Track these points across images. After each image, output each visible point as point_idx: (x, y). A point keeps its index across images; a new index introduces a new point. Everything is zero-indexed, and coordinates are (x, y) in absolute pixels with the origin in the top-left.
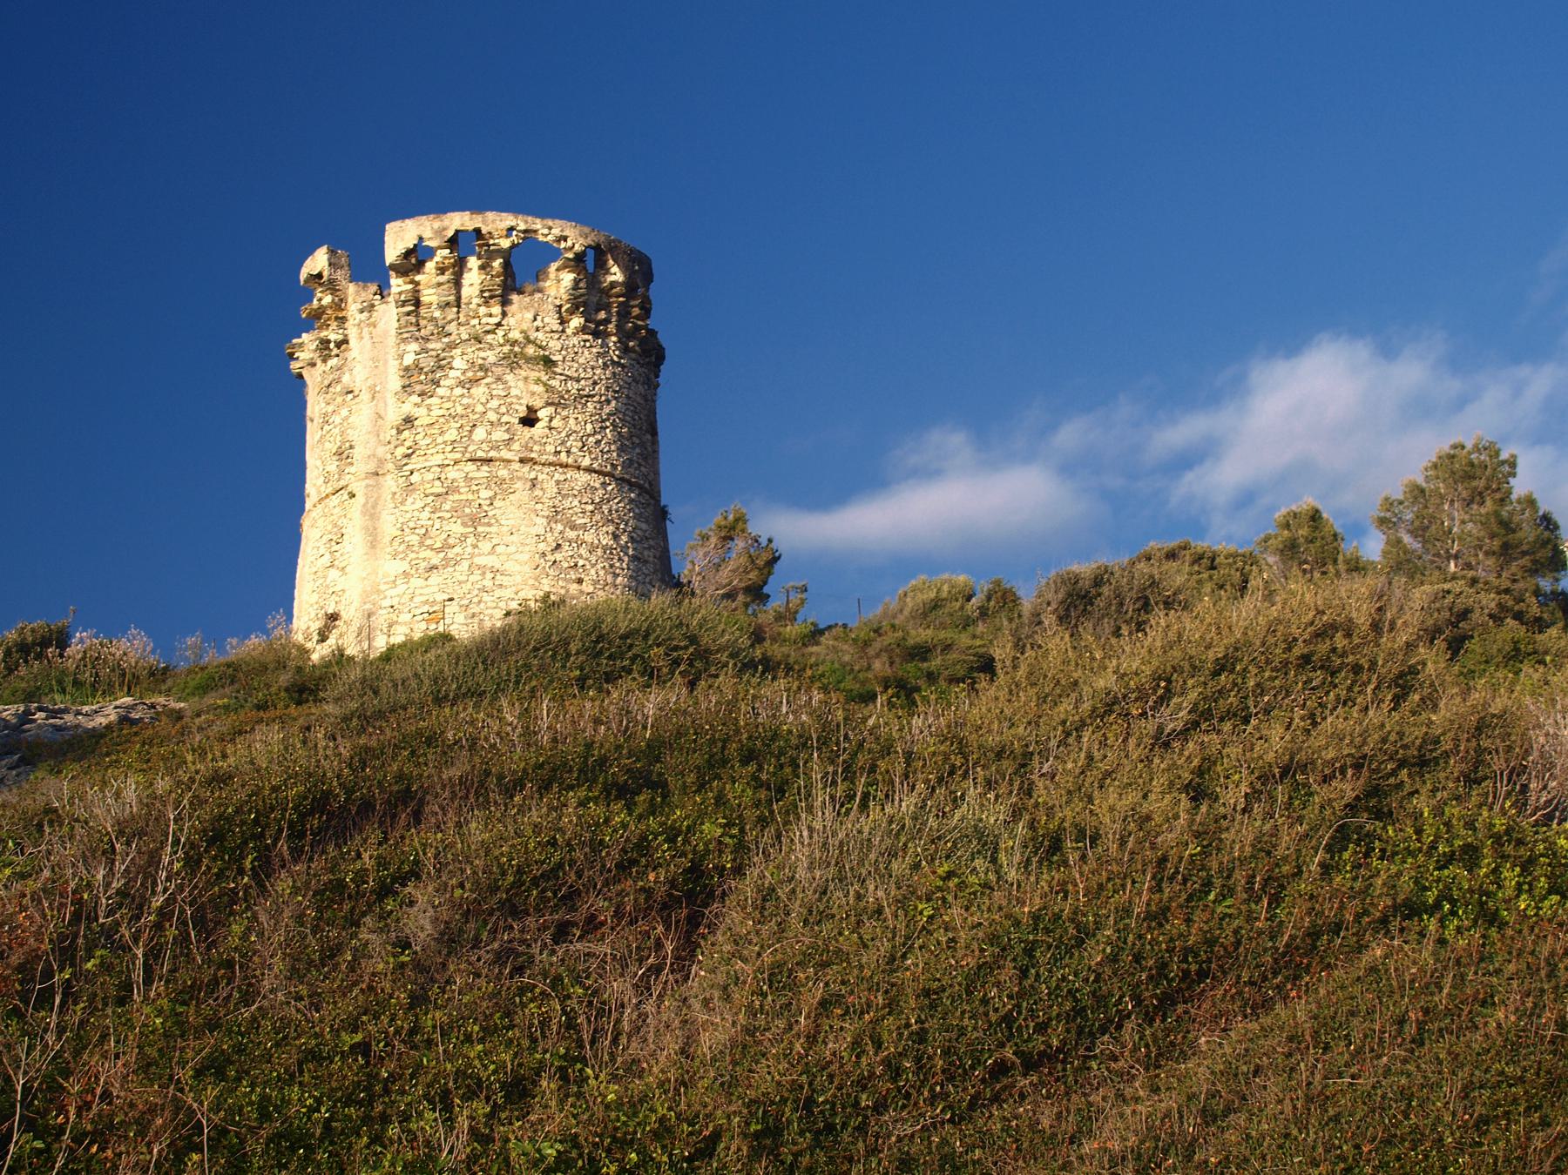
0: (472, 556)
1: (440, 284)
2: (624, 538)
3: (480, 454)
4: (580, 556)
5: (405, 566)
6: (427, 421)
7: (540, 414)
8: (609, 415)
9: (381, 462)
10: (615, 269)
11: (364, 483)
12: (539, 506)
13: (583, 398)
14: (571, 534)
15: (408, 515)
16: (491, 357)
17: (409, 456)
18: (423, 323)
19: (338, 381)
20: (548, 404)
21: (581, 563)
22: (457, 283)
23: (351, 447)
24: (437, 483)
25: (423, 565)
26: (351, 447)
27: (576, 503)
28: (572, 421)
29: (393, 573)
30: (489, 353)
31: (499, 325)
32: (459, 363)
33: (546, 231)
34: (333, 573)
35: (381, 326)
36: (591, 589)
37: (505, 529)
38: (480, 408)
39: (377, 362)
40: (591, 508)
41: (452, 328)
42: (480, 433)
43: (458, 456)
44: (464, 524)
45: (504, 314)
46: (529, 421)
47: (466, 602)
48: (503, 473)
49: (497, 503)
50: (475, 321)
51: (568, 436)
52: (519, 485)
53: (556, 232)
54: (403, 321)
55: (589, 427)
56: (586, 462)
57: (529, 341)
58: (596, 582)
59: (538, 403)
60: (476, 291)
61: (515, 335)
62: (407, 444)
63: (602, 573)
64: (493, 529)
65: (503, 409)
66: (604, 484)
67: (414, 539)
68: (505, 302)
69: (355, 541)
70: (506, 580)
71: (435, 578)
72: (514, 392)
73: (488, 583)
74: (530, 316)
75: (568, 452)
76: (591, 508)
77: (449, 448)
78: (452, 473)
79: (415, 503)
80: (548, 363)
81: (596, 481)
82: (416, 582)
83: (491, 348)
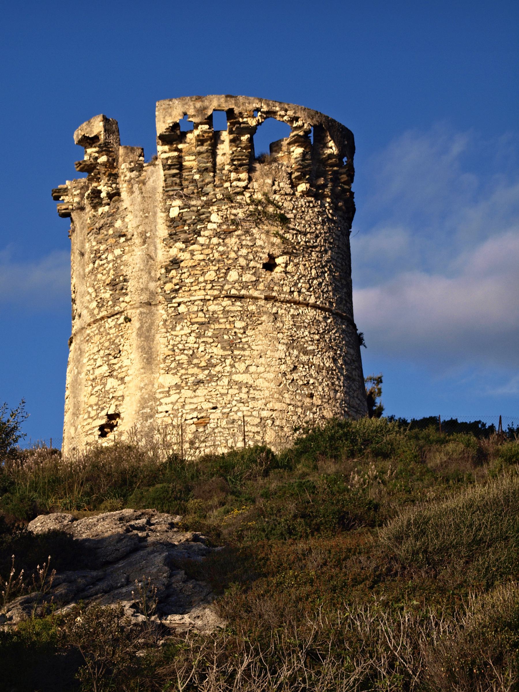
0: (231, 373)
1: (200, 153)
2: (340, 362)
3: (233, 292)
4: (311, 376)
5: (176, 380)
6: (191, 263)
7: (278, 261)
8: (327, 262)
9: (153, 294)
10: (331, 144)
11: (138, 311)
12: (280, 335)
13: (308, 248)
14: (304, 358)
15: (178, 339)
16: (240, 213)
17: (176, 291)
18: (185, 183)
19: (111, 225)
20: (284, 253)
21: (311, 381)
22: (214, 154)
23: (125, 280)
24: (201, 314)
25: (192, 379)
26: (125, 280)
27: (306, 333)
28: (301, 267)
29: (167, 385)
30: (239, 211)
31: (246, 188)
32: (214, 217)
33: (283, 113)
34: (111, 382)
35: (150, 183)
36: (319, 402)
37: (255, 353)
38: (233, 255)
39: (147, 214)
40: (317, 337)
41: (209, 188)
42: (233, 275)
43: (216, 293)
44: (224, 348)
45: (250, 179)
46: (270, 266)
47: (226, 410)
48: (252, 308)
49: (249, 332)
50: (227, 184)
51: (299, 279)
52: (264, 318)
53: (290, 113)
54: (169, 181)
55: (314, 272)
56: (312, 300)
57: (270, 202)
58: (322, 397)
59: (276, 252)
60: (227, 159)
61: (258, 196)
62: (175, 281)
63: (326, 389)
64: (247, 353)
65: (251, 257)
66: (325, 318)
67: (183, 358)
68: (251, 170)
69: (131, 359)
70: (257, 394)
71: (201, 391)
72: (259, 243)
73: (244, 396)
74: (269, 181)
75: (299, 292)
76: (317, 337)
77: (209, 286)
78: (213, 307)
79: (182, 330)
80: (284, 220)
81: (320, 316)
82: (186, 393)
83: (240, 206)
